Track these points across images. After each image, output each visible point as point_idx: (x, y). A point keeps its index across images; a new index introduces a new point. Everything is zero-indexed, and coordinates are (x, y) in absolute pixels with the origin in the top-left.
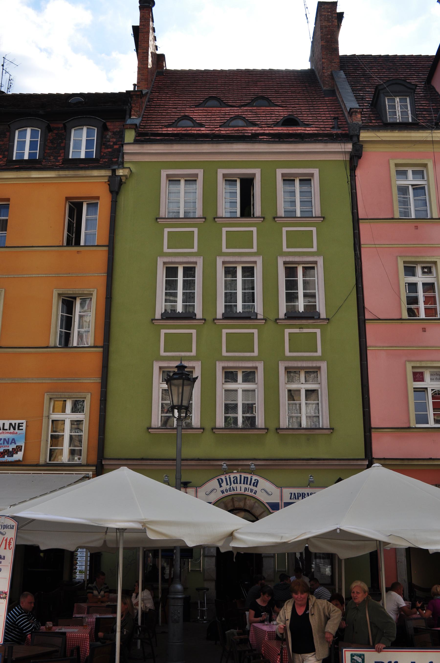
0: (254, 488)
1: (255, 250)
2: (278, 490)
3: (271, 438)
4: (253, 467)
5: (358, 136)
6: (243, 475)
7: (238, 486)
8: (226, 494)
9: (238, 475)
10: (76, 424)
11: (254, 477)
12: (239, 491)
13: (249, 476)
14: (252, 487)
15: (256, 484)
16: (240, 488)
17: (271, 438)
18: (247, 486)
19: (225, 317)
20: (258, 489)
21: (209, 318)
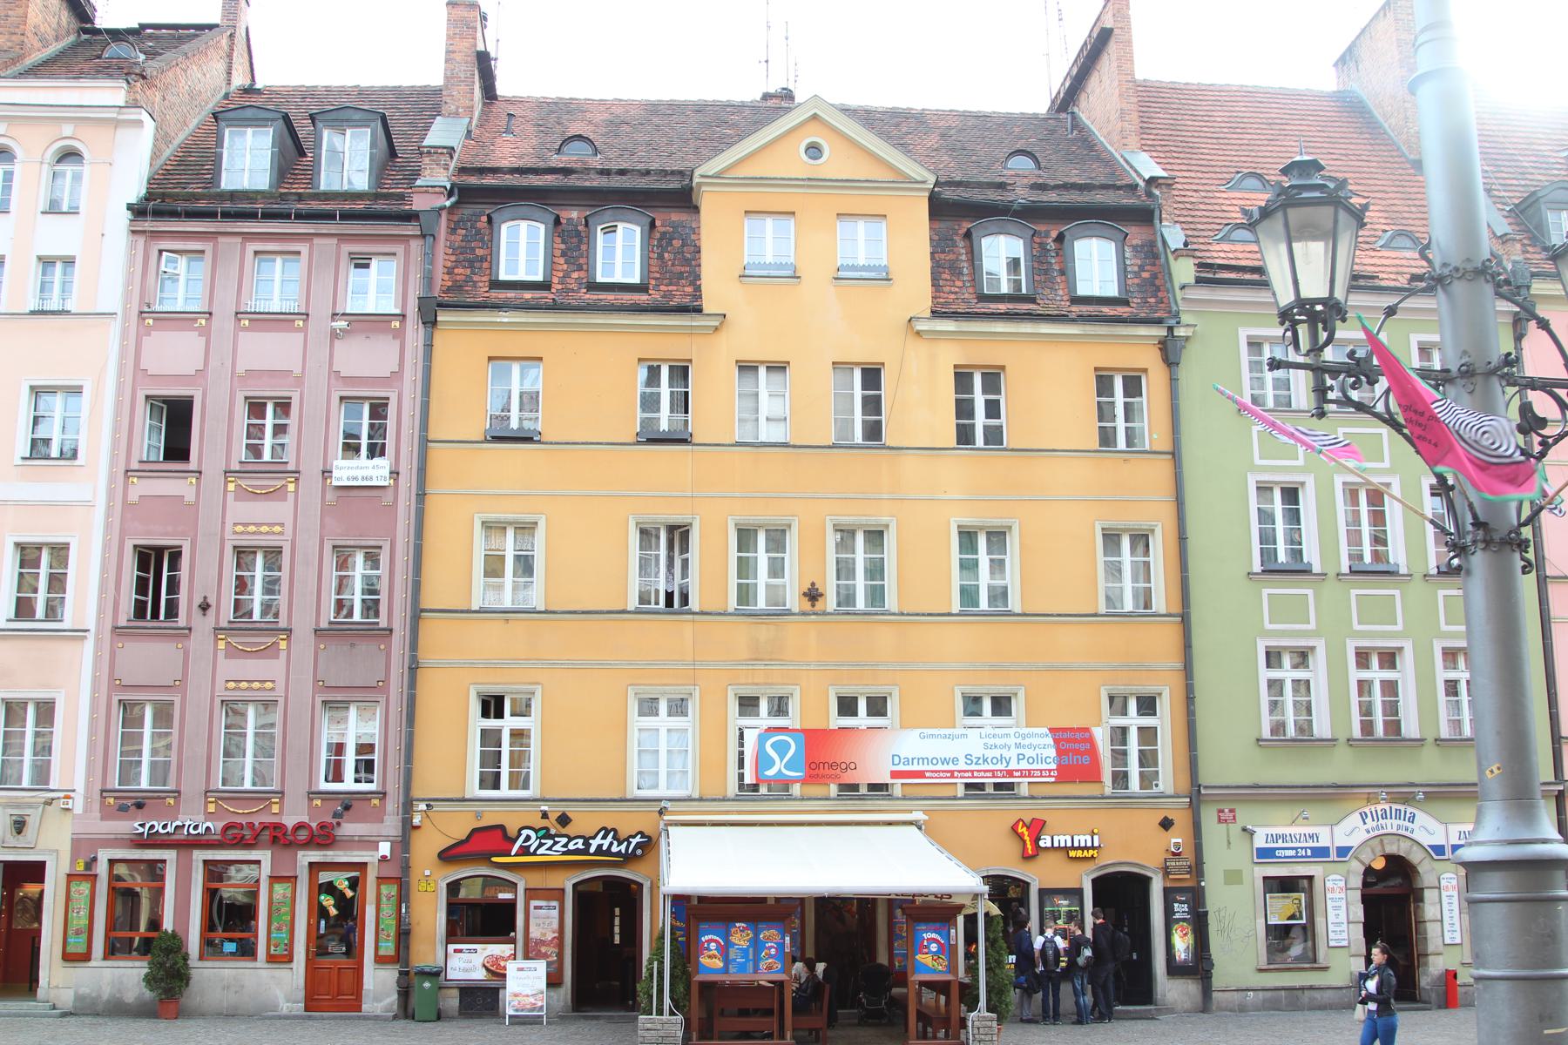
0: (1410, 825)
1: (1386, 464)
2: (1443, 827)
3: (1429, 752)
4: (1421, 796)
5: (1528, 287)
6: (1395, 807)
7: (1388, 821)
8: (1372, 834)
9: (1387, 807)
10: (1148, 735)
11: (1410, 810)
12: (1389, 830)
13: (1402, 808)
14: (1406, 823)
15: (1412, 819)
16: (1391, 825)
17: (1429, 752)
18: (1401, 822)
19: (1352, 572)
20: (1415, 826)
21: (1332, 573)
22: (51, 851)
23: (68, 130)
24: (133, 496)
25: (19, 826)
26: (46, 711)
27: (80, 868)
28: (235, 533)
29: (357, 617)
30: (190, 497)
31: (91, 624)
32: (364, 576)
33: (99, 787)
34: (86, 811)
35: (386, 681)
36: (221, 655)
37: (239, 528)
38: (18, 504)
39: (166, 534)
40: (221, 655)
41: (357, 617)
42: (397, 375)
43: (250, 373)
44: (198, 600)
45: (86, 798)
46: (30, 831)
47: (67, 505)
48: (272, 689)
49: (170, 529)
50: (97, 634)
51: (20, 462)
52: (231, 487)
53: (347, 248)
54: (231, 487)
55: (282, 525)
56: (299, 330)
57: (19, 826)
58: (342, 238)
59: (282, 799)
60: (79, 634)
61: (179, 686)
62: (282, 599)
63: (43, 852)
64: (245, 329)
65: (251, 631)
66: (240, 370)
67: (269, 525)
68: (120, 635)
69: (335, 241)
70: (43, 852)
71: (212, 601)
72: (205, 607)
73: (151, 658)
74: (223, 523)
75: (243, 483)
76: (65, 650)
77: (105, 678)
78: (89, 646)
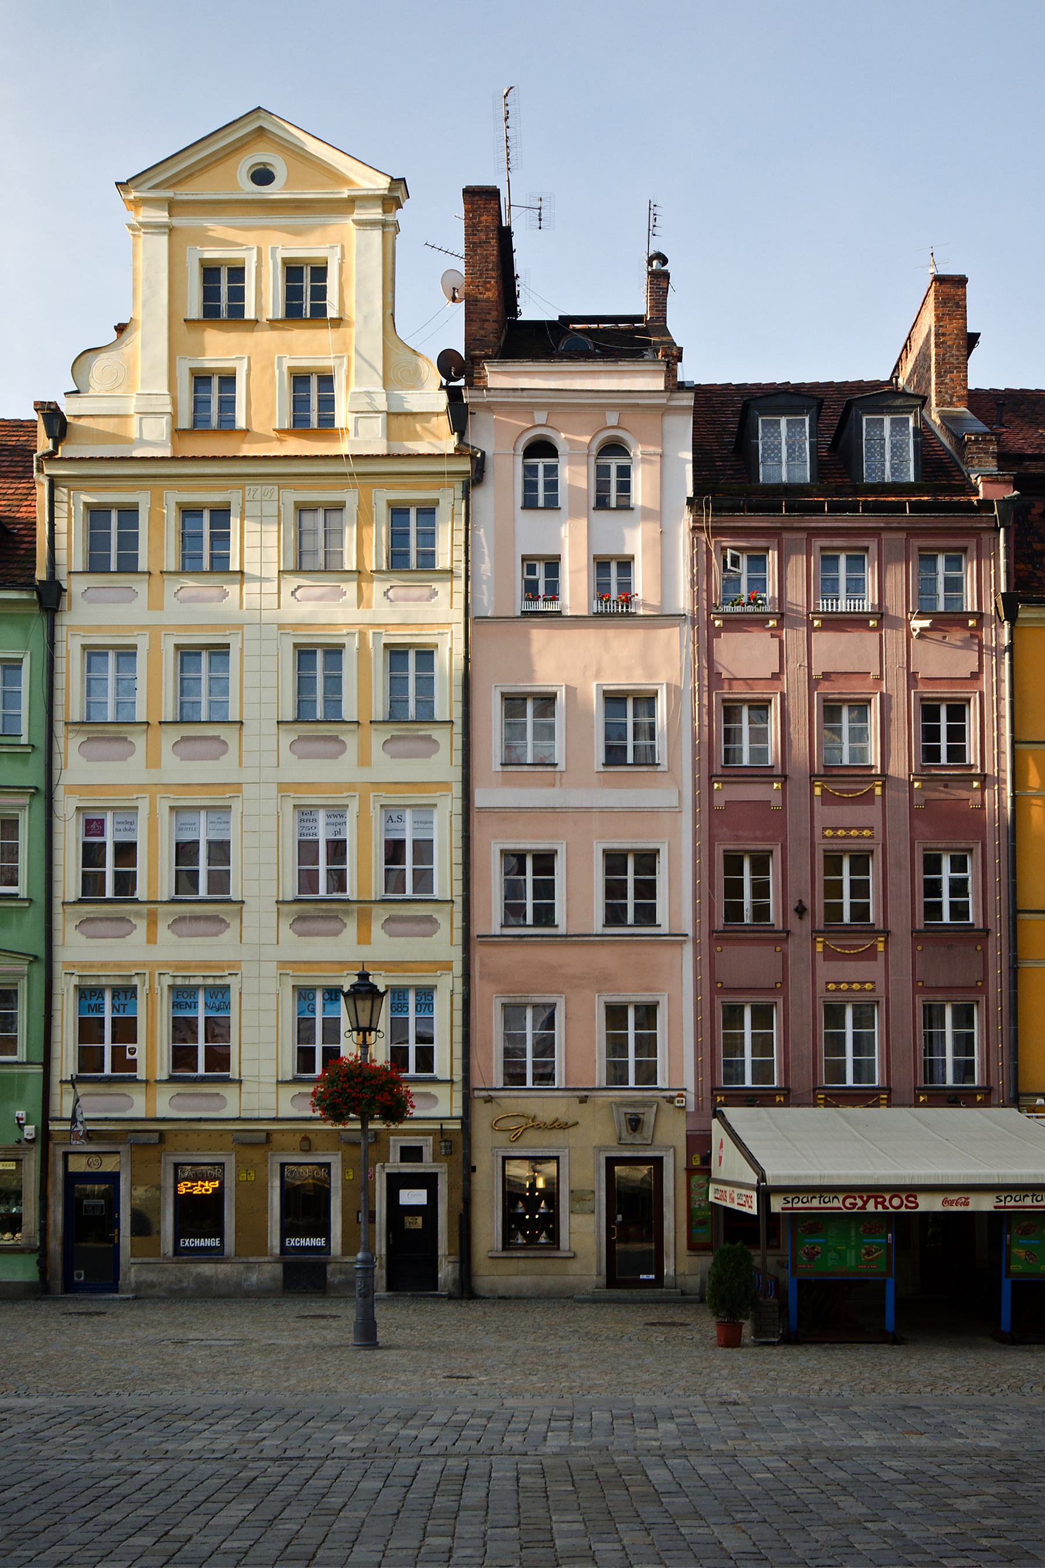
22: (667, 1148)
23: (612, 418)
24: (719, 802)
25: (635, 1123)
26: (648, 1014)
27: (696, 1162)
28: (825, 837)
29: (946, 919)
30: (776, 802)
31: (689, 930)
32: (951, 880)
33: (707, 1086)
34: (697, 1108)
35: (985, 979)
36: (819, 958)
37: (828, 833)
38: (603, 810)
39: (756, 839)
40: (819, 958)
41: (946, 919)
42: (976, 676)
43: (826, 676)
44: (792, 905)
45: (697, 1096)
46: (647, 1131)
47: (654, 811)
48: (873, 990)
49: (758, 833)
50: (695, 940)
51: (602, 769)
52: (818, 791)
53: (917, 543)
54: (818, 791)
55: (871, 829)
56: (873, 629)
57: (635, 1123)
58: (913, 532)
59: (889, 1095)
60: (675, 939)
61: (781, 988)
62: (873, 901)
63: (661, 1148)
64: (816, 629)
65: (850, 933)
66: (816, 672)
67: (858, 829)
68: (717, 939)
69: (903, 535)
70: (661, 1148)
71: (807, 904)
72: (801, 910)
73: (751, 963)
74: (812, 827)
75: (830, 788)
76: (665, 954)
77: (706, 983)
78: (688, 950)
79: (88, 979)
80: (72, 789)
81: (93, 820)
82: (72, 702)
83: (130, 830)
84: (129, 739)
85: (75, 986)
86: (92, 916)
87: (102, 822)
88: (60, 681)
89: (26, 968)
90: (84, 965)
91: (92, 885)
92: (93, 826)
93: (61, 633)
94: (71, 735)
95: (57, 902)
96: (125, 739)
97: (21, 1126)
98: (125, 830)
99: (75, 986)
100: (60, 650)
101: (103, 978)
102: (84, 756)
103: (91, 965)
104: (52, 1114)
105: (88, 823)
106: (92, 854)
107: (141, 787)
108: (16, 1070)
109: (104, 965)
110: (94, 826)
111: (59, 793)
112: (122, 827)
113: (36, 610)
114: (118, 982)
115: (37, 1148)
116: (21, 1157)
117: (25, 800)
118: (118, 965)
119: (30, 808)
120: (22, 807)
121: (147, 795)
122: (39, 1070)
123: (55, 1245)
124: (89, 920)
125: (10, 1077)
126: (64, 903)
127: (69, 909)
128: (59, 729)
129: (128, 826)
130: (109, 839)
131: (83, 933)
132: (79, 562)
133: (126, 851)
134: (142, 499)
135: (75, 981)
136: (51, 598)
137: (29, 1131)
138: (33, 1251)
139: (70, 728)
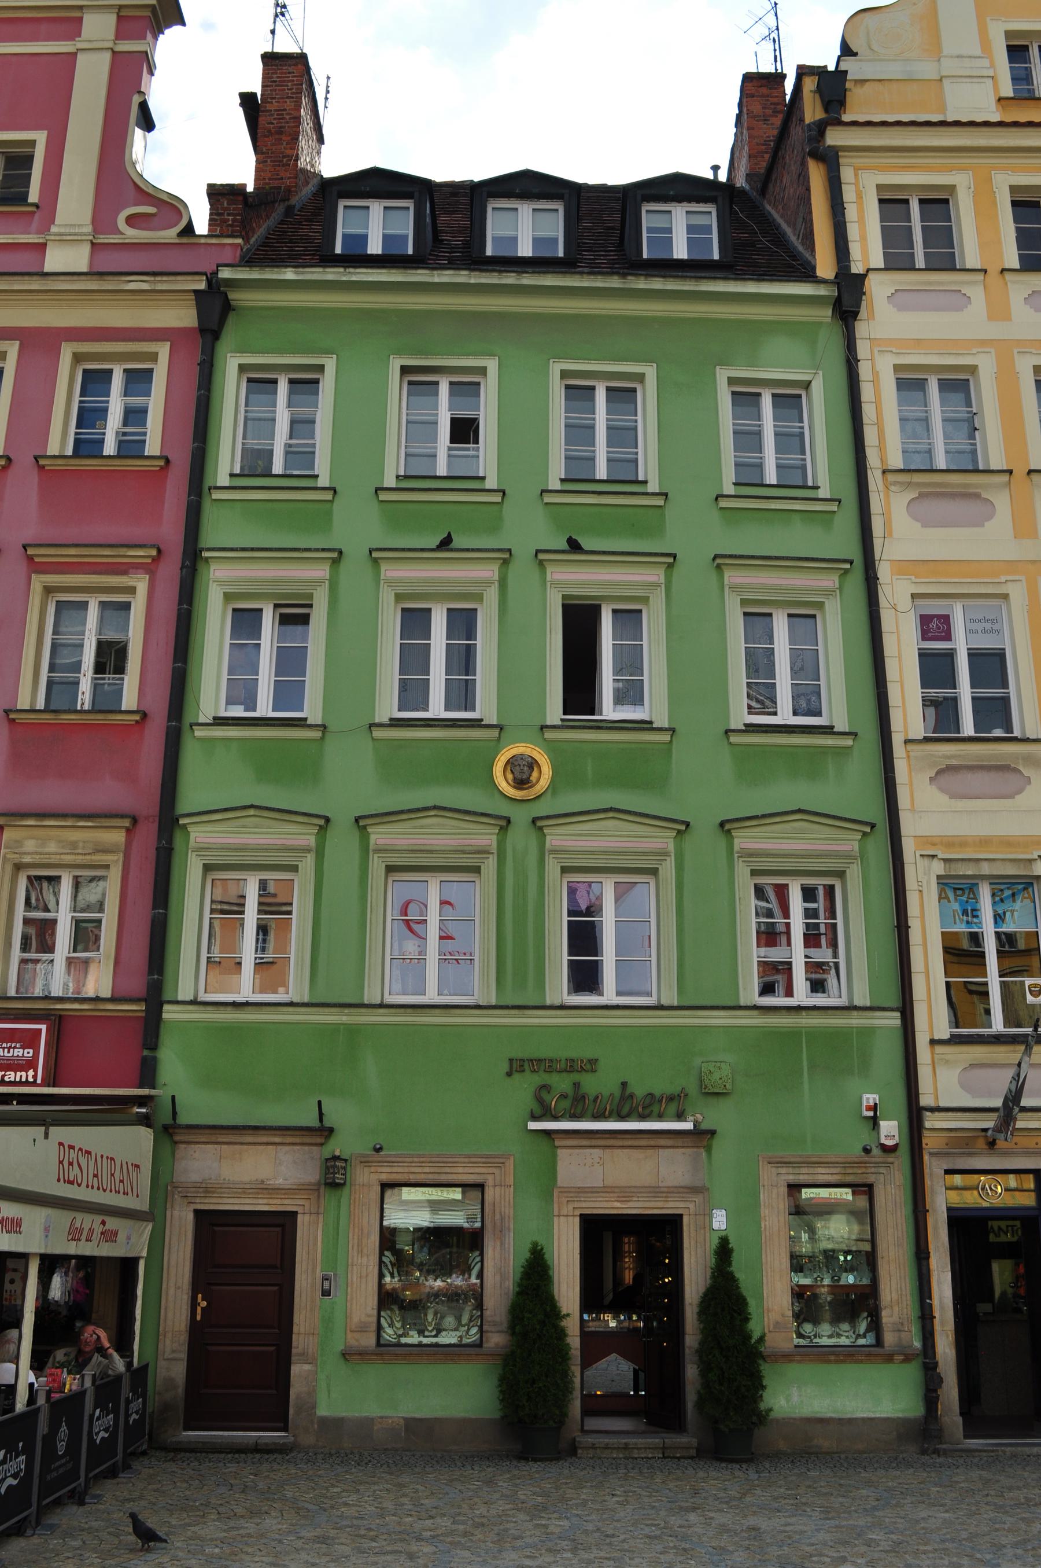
79: (959, 865)
80: (904, 567)
81: (932, 617)
82: (887, 442)
83: (992, 631)
84: (984, 495)
85: (939, 877)
86: (954, 762)
87: (946, 619)
88: (868, 412)
89: (856, 846)
90: (949, 843)
91: (943, 713)
92: (933, 625)
93: (863, 350)
94: (893, 488)
95: (897, 740)
96: (977, 496)
97: (874, 1121)
98: (984, 631)
99: (939, 877)
100: (864, 371)
101: (985, 865)
102: (917, 520)
103: (962, 842)
104: (925, 1100)
105: (925, 620)
106: (936, 668)
107: (1011, 566)
108: (855, 1020)
109: (984, 842)
110: (934, 626)
111: (884, 572)
112: (979, 627)
113: (826, 313)
114: (1011, 870)
115: (902, 1161)
116: (871, 1179)
117: (830, 581)
118: (1007, 842)
119: (841, 592)
120: (828, 592)
121: (1023, 578)
122: (893, 1020)
123: (945, 1347)
124: (950, 769)
125: (841, 1036)
126: (907, 742)
127: (917, 750)
128: (875, 480)
129: (988, 626)
130: (961, 644)
131: (942, 790)
132: (877, 259)
133: (990, 665)
134: (962, 182)
135: (938, 868)
136: (848, 298)
137: (890, 1130)
138: (908, 1359)
139: (891, 477)
